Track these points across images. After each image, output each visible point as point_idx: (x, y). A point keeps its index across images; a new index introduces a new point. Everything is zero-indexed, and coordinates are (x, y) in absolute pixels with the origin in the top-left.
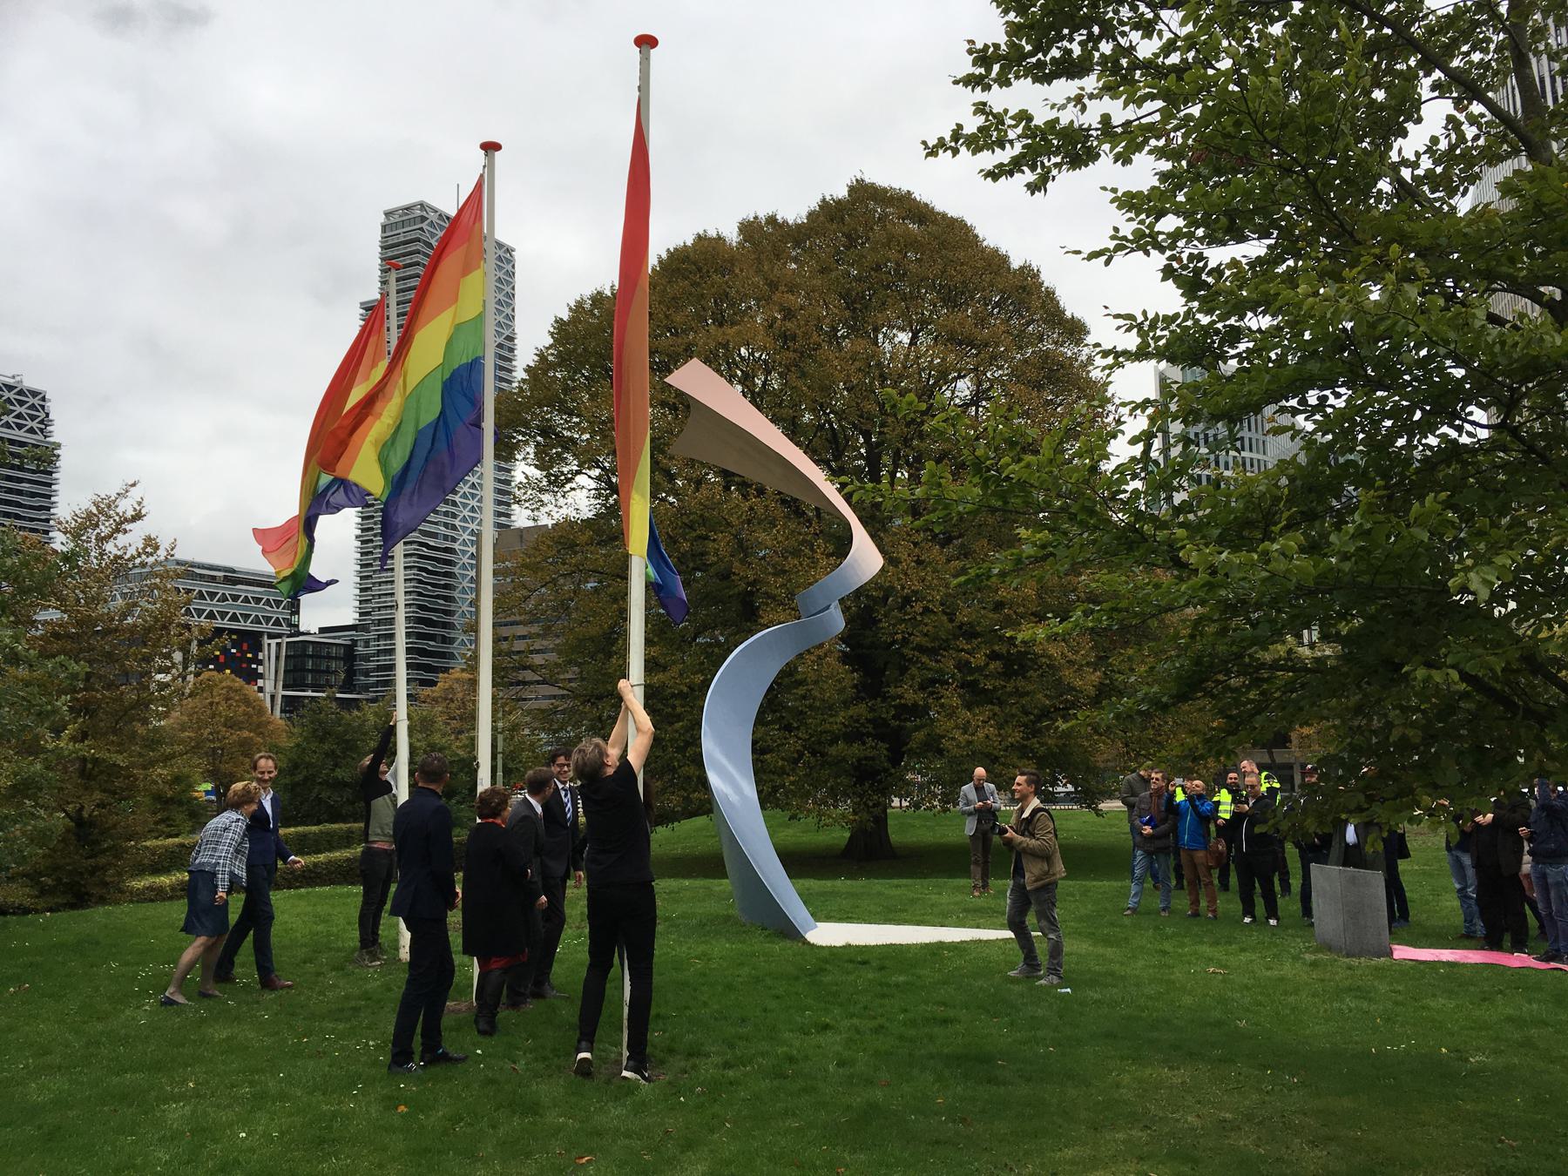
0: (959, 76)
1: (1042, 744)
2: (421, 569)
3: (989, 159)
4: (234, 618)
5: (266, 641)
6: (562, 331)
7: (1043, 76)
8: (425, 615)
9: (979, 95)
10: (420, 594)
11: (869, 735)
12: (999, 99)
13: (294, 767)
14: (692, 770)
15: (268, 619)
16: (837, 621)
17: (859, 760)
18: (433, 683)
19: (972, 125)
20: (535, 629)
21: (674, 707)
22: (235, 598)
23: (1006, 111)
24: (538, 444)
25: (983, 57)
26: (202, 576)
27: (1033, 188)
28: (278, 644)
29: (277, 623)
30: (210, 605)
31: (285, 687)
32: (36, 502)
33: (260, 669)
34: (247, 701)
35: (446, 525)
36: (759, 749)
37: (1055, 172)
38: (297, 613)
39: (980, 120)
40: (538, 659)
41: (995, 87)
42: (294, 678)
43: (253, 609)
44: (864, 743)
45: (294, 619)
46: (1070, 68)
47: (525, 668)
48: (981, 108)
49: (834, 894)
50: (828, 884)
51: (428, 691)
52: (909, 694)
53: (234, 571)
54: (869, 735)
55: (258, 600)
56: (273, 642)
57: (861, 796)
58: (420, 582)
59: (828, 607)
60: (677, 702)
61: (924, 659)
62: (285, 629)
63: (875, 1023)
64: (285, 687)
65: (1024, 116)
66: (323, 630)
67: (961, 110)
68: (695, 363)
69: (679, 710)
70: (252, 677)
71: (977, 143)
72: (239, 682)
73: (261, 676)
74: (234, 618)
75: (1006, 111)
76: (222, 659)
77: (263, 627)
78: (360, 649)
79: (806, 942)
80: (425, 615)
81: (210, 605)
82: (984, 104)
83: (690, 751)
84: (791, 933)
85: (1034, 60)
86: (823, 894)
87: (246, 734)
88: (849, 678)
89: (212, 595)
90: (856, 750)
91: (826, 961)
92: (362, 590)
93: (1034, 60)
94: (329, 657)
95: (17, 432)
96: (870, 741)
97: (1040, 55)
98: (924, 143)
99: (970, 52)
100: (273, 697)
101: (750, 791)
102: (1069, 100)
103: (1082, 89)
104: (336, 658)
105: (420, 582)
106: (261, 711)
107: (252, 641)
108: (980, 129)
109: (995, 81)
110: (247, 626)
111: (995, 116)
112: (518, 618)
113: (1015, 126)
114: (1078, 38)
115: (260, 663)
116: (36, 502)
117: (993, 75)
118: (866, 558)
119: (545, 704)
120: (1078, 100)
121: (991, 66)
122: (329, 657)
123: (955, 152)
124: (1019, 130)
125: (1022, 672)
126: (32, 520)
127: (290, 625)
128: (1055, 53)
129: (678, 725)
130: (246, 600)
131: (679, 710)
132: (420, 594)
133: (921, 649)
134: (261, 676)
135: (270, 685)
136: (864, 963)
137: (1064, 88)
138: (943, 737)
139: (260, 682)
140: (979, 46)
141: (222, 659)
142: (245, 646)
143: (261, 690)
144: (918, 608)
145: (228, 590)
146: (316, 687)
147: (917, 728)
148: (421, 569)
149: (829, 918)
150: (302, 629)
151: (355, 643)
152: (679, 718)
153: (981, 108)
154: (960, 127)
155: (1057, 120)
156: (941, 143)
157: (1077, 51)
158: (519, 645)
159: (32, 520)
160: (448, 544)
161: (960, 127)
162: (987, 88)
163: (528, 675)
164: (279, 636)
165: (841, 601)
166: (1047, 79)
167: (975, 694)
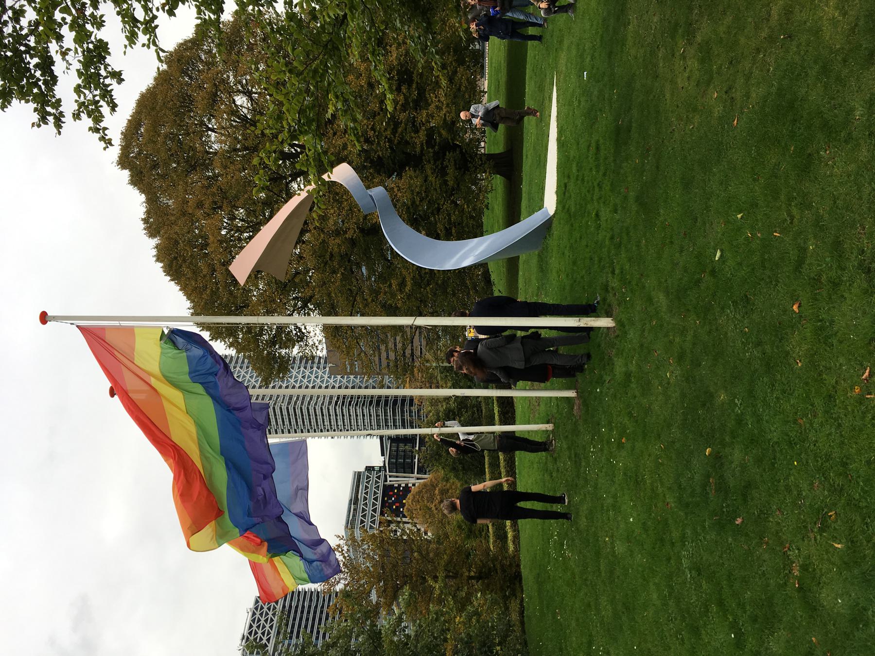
2: (350, 404)
3: (105, 109)
5: (388, 483)
7: (53, 80)
9: (68, 118)
10: (363, 405)
13: (454, 469)
15: (377, 482)
19: (86, 121)
20: (383, 348)
22: (365, 499)
24: (280, 348)
26: (354, 516)
27: (120, 81)
28: (390, 476)
29: (379, 477)
31: (413, 473)
33: (403, 485)
34: (420, 492)
37: (110, 69)
38: (373, 467)
40: (399, 346)
41: (61, 109)
42: (408, 468)
43: (371, 490)
45: (376, 469)
46: (47, 64)
47: (404, 353)
48: (77, 116)
49: (529, 193)
50: (524, 196)
55: (367, 487)
56: (389, 479)
58: (357, 405)
61: (400, 130)
62: (382, 474)
64: (413, 473)
65: (78, 90)
66: (383, 454)
67: (78, 129)
68: (231, 268)
70: (407, 489)
71: (97, 117)
72: (410, 496)
73: (407, 485)
74: (376, 499)
75: (76, 101)
76: (398, 505)
77: (381, 484)
81: (369, 511)
85: (43, 87)
87: (437, 492)
88: (409, 172)
89: (364, 510)
93: (43, 87)
94: (397, 451)
95: (275, 622)
97: (40, 83)
100: (418, 479)
102: (64, 59)
103: (57, 52)
104: (398, 447)
105: (357, 405)
106: (425, 485)
107: (388, 489)
109: (57, 109)
110: (380, 495)
112: (377, 359)
113: (85, 95)
114: (28, 58)
115: (400, 485)
119: (424, 343)
120: (64, 54)
121: (47, 108)
122: (397, 451)
125: (409, 73)
127: (380, 471)
128: (38, 74)
130: (366, 493)
133: (394, 132)
134: (407, 485)
135: (412, 480)
136: (566, 187)
137: (58, 68)
138: (445, 119)
139: (410, 485)
141: (398, 505)
143: (414, 485)
144: (371, 133)
145: (361, 503)
146: (413, 458)
148: (350, 404)
150: (382, 465)
155: (78, 71)
157: (36, 60)
158: (392, 355)
162: (61, 114)
163: (408, 352)
164: (386, 476)
166: (54, 79)
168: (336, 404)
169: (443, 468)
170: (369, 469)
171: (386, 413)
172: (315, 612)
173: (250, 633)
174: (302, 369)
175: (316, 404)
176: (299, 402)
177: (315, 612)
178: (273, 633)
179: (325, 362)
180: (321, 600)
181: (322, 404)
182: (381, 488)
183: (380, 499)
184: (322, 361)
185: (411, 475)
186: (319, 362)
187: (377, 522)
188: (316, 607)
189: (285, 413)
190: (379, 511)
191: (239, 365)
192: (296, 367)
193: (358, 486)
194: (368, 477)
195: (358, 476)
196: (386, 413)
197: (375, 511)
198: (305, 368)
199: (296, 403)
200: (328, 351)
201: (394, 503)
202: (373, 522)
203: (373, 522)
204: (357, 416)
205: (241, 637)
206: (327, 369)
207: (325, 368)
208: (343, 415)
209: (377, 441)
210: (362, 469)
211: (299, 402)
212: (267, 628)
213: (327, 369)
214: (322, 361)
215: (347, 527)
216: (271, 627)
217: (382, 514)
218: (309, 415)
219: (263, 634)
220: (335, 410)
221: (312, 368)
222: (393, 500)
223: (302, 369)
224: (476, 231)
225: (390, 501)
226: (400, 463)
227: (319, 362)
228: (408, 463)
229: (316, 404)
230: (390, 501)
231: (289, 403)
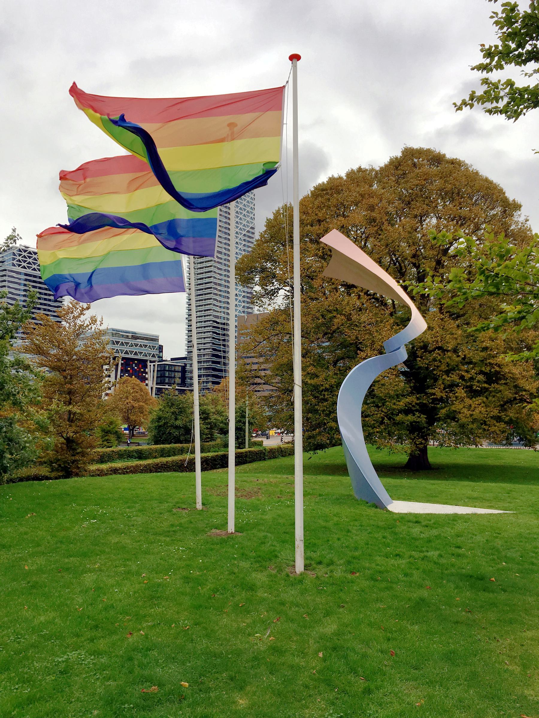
0: (474, 65)
1: (507, 416)
4: (136, 354)
5: (149, 364)
6: (270, 225)
8: (216, 353)
11: (417, 410)
12: (495, 76)
14: (333, 424)
16: (404, 355)
17: (411, 423)
18: (218, 383)
20: (261, 360)
21: (324, 395)
23: (499, 81)
25: (489, 54)
26: (123, 336)
28: (154, 365)
29: (153, 356)
33: (147, 376)
34: (141, 390)
35: (224, 313)
36: (364, 415)
39: (485, 87)
40: (262, 373)
42: (161, 379)
43: (144, 350)
44: (414, 415)
47: (256, 377)
51: (216, 386)
52: (438, 392)
53: (136, 334)
54: (417, 410)
55: (146, 346)
57: (413, 440)
59: (399, 348)
60: (326, 393)
62: (157, 359)
63: (422, 555)
64: (157, 384)
69: (326, 396)
70: (144, 379)
72: (138, 381)
73: (147, 379)
76: (131, 372)
77: (149, 358)
78: (188, 368)
79: (388, 511)
80: (216, 353)
81: (128, 348)
82: (487, 79)
83: (332, 416)
84: (378, 505)
86: (396, 486)
87: (141, 404)
90: (410, 417)
91: (395, 520)
92: (189, 342)
94: (175, 371)
96: (417, 414)
98: (454, 104)
99: (482, 51)
100: (152, 388)
101: (361, 436)
104: (178, 372)
105: (213, 338)
106: (147, 393)
107: (143, 363)
108: (485, 92)
110: (139, 357)
111: (493, 85)
112: (253, 355)
115: (146, 373)
117: (494, 63)
118: (418, 324)
119: (266, 394)
122: (175, 371)
123: (472, 106)
124: (507, 90)
127: (159, 357)
129: (325, 404)
130: (141, 346)
131: (326, 396)
132: (213, 344)
134: (147, 379)
135: (151, 383)
139: (147, 382)
140: (487, 47)
142: (140, 367)
143: (147, 385)
145: (134, 342)
146: (170, 384)
147: (442, 408)
149: (399, 499)
150: (164, 359)
151: (186, 365)
152: (326, 400)
153: (485, 81)
154: (474, 92)
156: (464, 103)
158: (255, 367)
160: (225, 321)
161: (474, 92)
163: (258, 380)
164: (154, 362)
165: (406, 345)
167: (473, 393)
168: (214, 321)
169: (160, 409)
170: (161, 348)
171: (207, 362)
172: (45, 305)
173: (30, 253)
174: (243, 294)
175: (214, 305)
176: (216, 292)
177: (45, 305)
178: (29, 271)
179: (249, 313)
181: (214, 310)
182: (145, 358)
183: (136, 357)
184: (250, 310)
185: (155, 383)
186: (248, 308)
187: (117, 355)
189: (207, 280)
190: (126, 356)
191: (247, 244)
192: (246, 289)
193: (147, 339)
194: (154, 347)
195: (155, 339)
196: (207, 362)
197: (126, 353)
198: (244, 297)
199: (216, 289)
200: (257, 315)
201: (133, 368)
203: (117, 351)
204: (204, 338)
205: (27, 245)
206: (243, 314)
207: (244, 312)
208: (205, 327)
209: (183, 354)
210: (160, 343)
211: (216, 292)
212: (33, 266)
213: (243, 314)
214: (250, 310)
215: (113, 330)
216: (34, 269)
217: (123, 359)
218: (205, 300)
219: (29, 263)
220: (209, 321)
221: (244, 302)
222: (134, 367)
223: (243, 294)
224: (369, 438)
225: (134, 365)
226: (165, 374)
227: (248, 308)
228: (165, 380)
229: (214, 305)
230: (134, 365)
231: (215, 284)
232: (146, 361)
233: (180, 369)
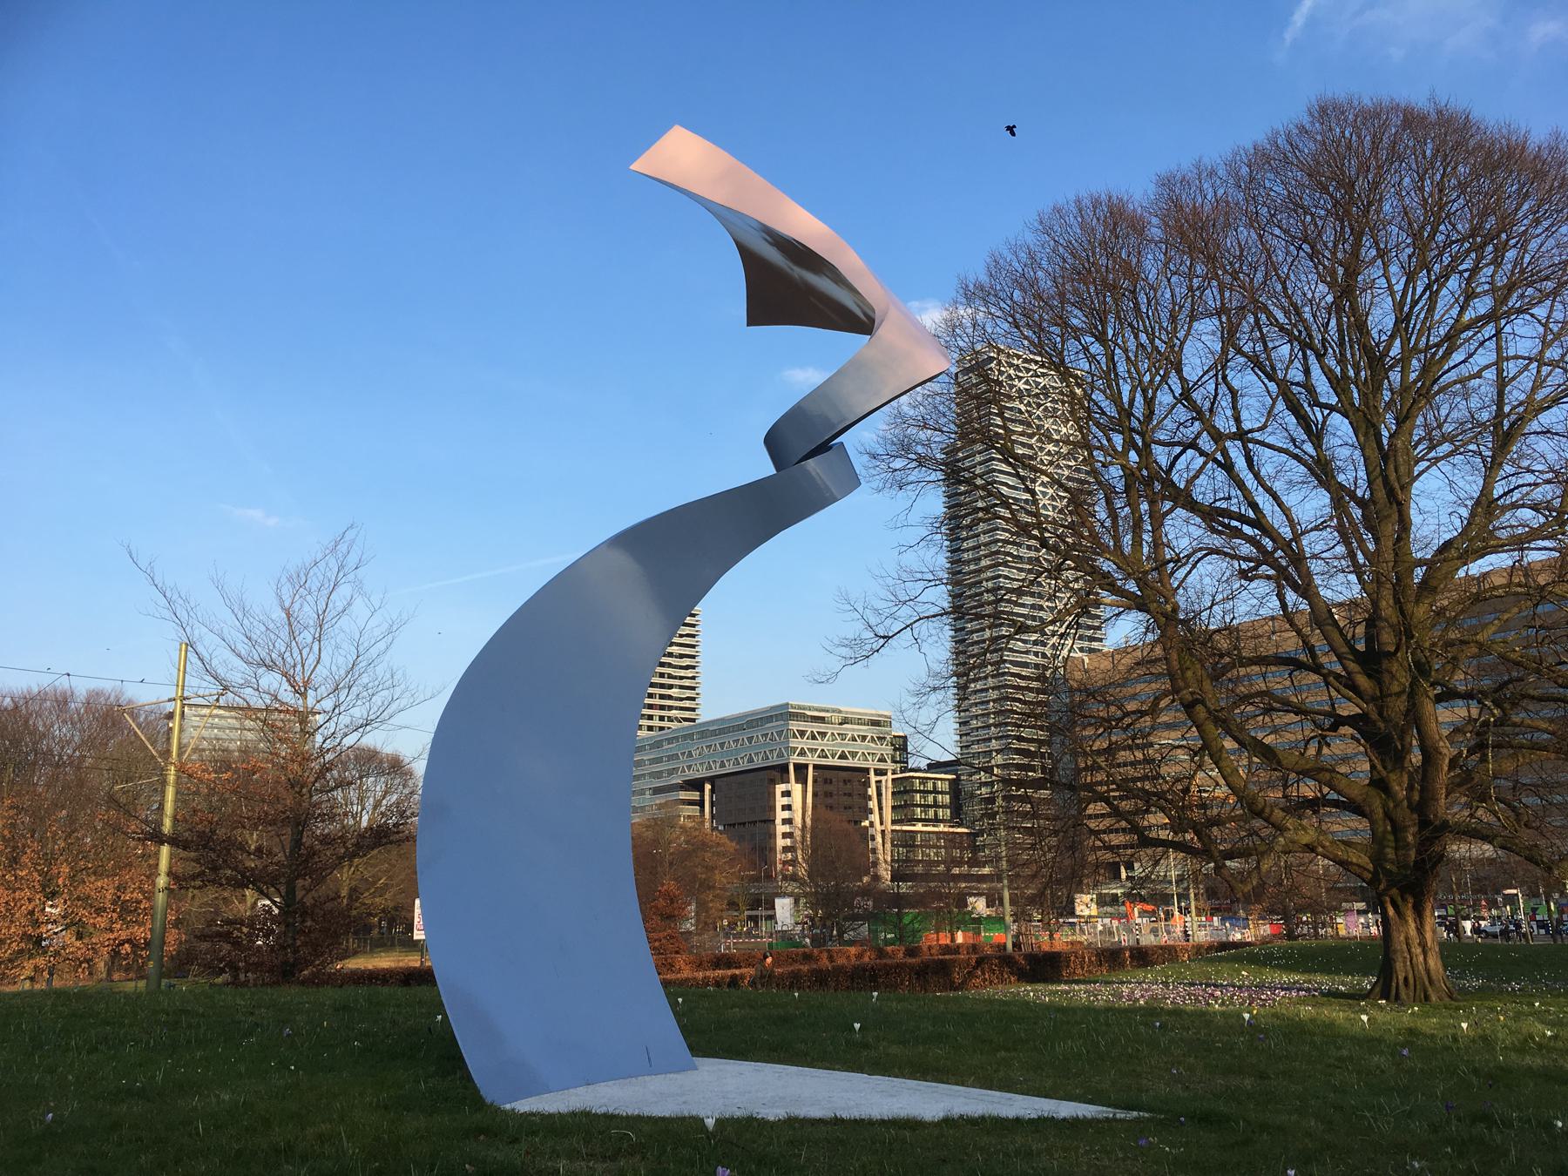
5: (873, 778)
29: (882, 760)
30: (819, 744)
31: (894, 822)
32: (686, 662)
35: (1036, 654)
55: (864, 738)
74: (843, 756)
77: (872, 764)
116: (686, 662)
126: (681, 678)
159: (681, 678)
180: (682, 673)
182: (864, 765)
183: (843, 763)
187: (802, 760)
188: (670, 665)
190: (823, 762)
202: (803, 753)
217: (816, 767)
232: (867, 770)
233: (946, 787)
